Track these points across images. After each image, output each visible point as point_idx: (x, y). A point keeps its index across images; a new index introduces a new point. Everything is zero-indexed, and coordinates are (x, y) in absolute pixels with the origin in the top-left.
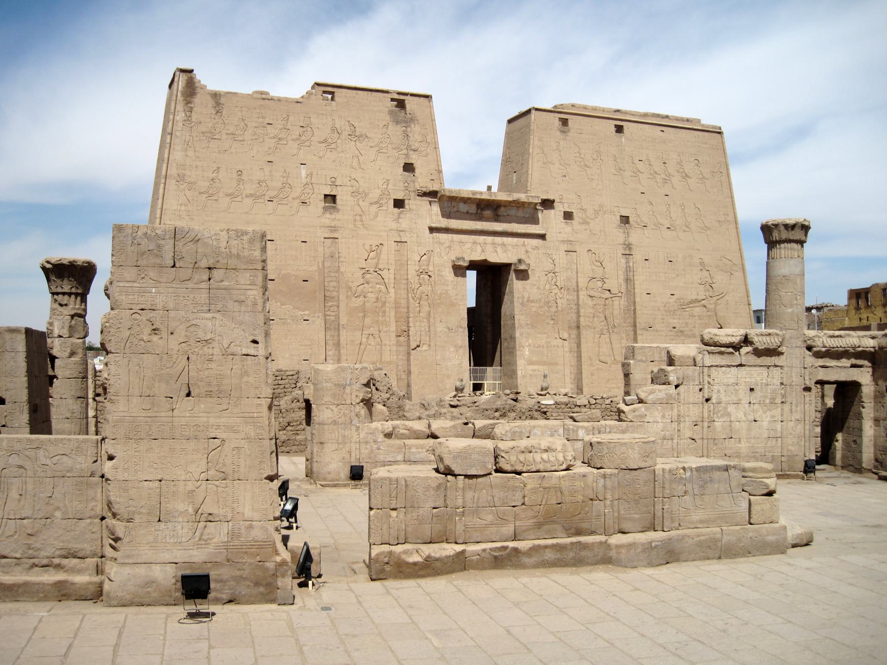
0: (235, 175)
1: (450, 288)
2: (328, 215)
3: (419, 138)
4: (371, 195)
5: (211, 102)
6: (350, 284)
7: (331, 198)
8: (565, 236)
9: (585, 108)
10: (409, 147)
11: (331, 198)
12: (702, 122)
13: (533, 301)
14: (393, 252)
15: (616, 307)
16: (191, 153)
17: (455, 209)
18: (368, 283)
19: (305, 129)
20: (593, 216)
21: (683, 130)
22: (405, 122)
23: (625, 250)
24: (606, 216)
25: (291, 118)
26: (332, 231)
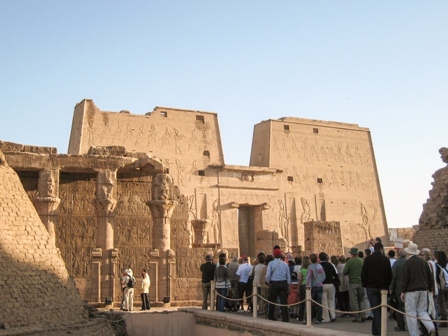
5: (101, 117)
9: (298, 119)
10: (205, 142)
12: (359, 126)
19: (152, 132)
20: (303, 179)
22: (204, 128)
23: (320, 197)
25: (144, 126)
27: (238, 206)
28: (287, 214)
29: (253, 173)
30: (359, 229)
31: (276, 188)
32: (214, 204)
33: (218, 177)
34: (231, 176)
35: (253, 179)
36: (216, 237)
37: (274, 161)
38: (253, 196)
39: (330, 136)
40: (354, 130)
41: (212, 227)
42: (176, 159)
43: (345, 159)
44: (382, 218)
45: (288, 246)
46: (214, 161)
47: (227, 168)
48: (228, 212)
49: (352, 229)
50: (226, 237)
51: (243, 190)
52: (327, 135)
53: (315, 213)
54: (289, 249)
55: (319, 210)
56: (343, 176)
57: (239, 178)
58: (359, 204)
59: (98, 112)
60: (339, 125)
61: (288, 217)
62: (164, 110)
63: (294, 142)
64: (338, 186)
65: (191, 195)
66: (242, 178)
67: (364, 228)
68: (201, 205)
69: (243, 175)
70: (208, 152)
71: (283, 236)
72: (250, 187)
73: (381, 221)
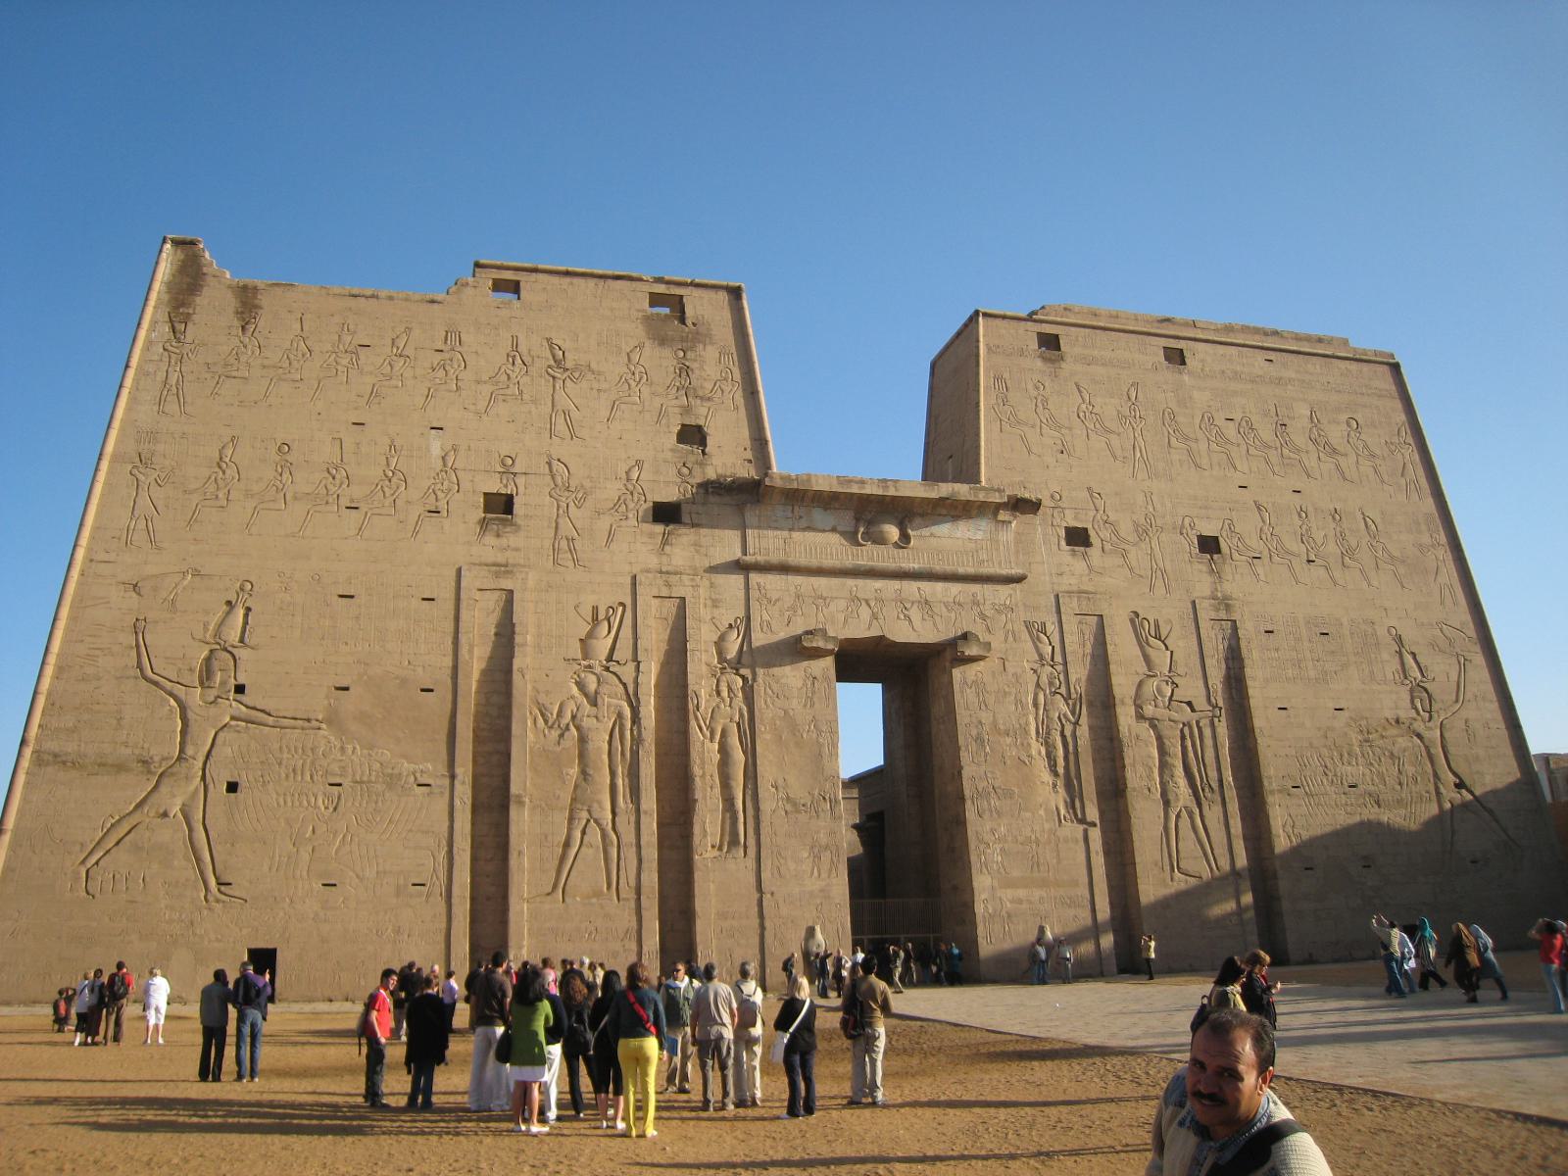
0: (274, 456)
1: (795, 702)
2: (490, 539)
5: (231, 302)
6: (542, 699)
7: (501, 506)
11: (501, 506)
12: (1353, 343)
14: (652, 622)
15: (1209, 742)
16: (172, 407)
18: (586, 695)
19: (446, 356)
20: (1133, 538)
21: (1315, 358)
22: (683, 340)
24: (1164, 537)
25: (416, 333)
26: (497, 575)
27: (830, 646)
28: (1073, 678)
29: (906, 512)
30: (1400, 740)
31: (1016, 571)
32: (722, 638)
33: (743, 528)
34: (804, 523)
35: (905, 537)
36: (733, 784)
37: (999, 464)
38: (908, 606)
39: (1236, 376)
41: (712, 740)
42: (550, 456)
43: (1311, 462)
44: (1492, 694)
45: (1082, 821)
46: (724, 464)
47: (778, 483)
48: (792, 675)
49: (1367, 741)
50: (780, 782)
51: (860, 582)
52: (1223, 372)
53: (1200, 674)
54: (1086, 832)
55: (1214, 661)
56: (1309, 529)
57: (843, 534)
58: (1389, 639)
59: (219, 282)
60: (1270, 338)
61: (1074, 696)
64: (1290, 568)
65: (613, 600)
66: (856, 533)
67: (1419, 736)
68: (664, 647)
69: (858, 520)
70: (699, 428)
71: (1056, 774)
72: (890, 565)
73: (1492, 709)
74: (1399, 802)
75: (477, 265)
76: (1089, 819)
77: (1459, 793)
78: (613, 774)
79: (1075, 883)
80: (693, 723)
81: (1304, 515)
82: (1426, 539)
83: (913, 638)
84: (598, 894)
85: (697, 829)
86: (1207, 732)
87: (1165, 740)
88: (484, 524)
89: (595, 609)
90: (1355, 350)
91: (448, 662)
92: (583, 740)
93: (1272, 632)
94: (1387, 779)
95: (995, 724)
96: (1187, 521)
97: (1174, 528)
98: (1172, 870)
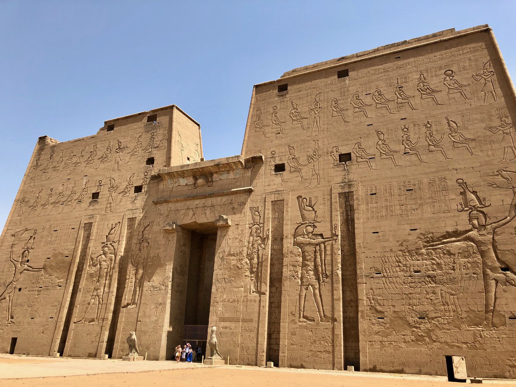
2: (91, 207)
3: (160, 138)
4: (121, 187)
6: (93, 256)
7: (95, 196)
8: (274, 187)
11: (95, 196)
13: (233, 255)
15: (329, 252)
17: (177, 184)
20: (307, 162)
23: (343, 188)
24: (321, 159)
28: (266, 229)
40: (441, 41)
43: (416, 101)
52: (369, 72)
62: (112, 123)
63: (295, 106)
65: (117, 222)
74: (452, 280)
75: (105, 123)
76: (262, 291)
77: (503, 274)
78: (106, 279)
79: (251, 321)
80: (130, 261)
81: (406, 130)
82: (496, 123)
83: (205, 221)
84: (93, 320)
85: (123, 297)
86: (329, 248)
87: (306, 254)
88: (90, 203)
89: (112, 225)
90: (459, 33)
91: (73, 247)
92: (101, 268)
93: (375, 194)
94: (443, 266)
95: (230, 251)
96: (334, 149)
97: (327, 153)
98: (300, 317)
